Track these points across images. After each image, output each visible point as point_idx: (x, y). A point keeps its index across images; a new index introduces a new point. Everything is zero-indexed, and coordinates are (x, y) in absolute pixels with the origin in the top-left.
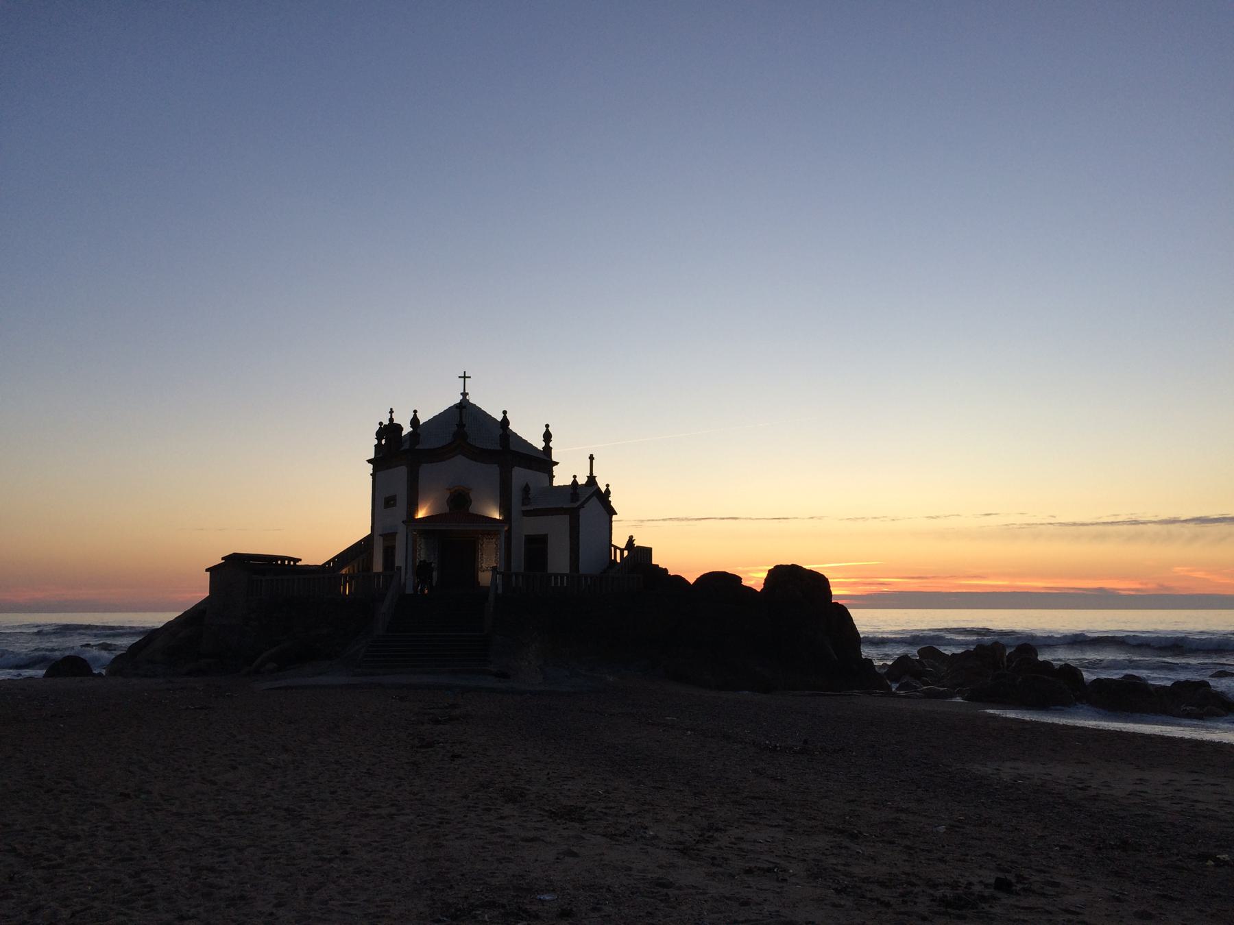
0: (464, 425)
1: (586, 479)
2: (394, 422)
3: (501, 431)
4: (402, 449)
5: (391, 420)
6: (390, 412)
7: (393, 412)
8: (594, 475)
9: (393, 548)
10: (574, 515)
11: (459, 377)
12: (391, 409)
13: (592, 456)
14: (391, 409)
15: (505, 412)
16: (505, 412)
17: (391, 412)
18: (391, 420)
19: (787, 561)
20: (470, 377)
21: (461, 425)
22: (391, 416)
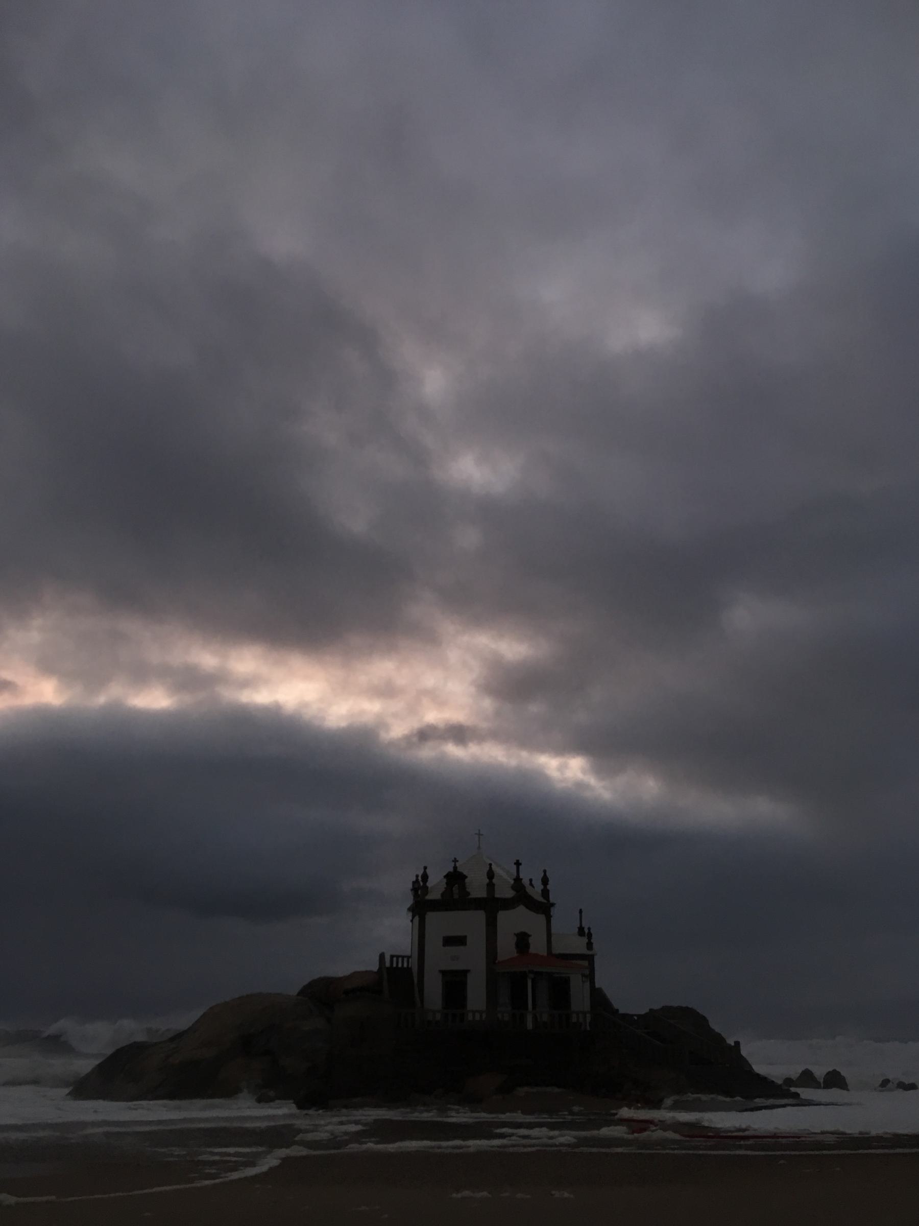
0: (522, 879)
1: (577, 930)
2: (459, 870)
3: (542, 887)
4: (470, 897)
5: (455, 868)
6: (453, 861)
7: (458, 861)
8: (583, 926)
9: (464, 985)
10: (590, 959)
11: (476, 834)
12: (455, 859)
13: (581, 911)
14: (455, 859)
15: (545, 871)
16: (545, 871)
17: (455, 861)
18: (455, 868)
19: (676, 1002)
20: (482, 835)
21: (518, 880)
22: (455, 865)
